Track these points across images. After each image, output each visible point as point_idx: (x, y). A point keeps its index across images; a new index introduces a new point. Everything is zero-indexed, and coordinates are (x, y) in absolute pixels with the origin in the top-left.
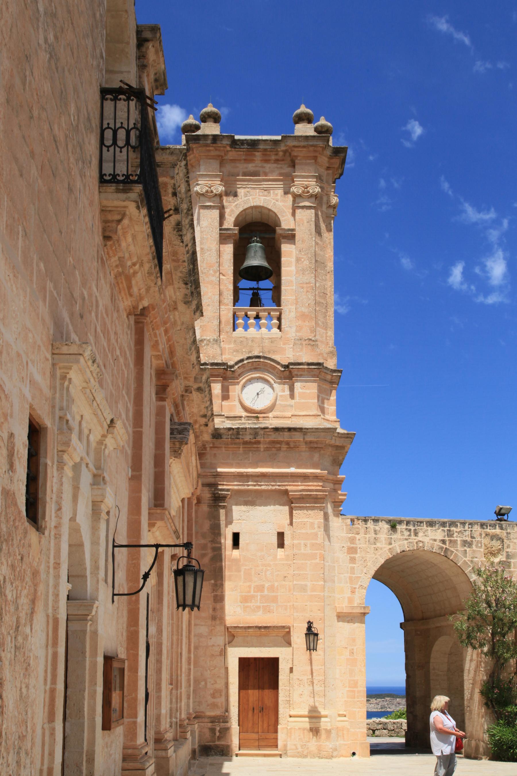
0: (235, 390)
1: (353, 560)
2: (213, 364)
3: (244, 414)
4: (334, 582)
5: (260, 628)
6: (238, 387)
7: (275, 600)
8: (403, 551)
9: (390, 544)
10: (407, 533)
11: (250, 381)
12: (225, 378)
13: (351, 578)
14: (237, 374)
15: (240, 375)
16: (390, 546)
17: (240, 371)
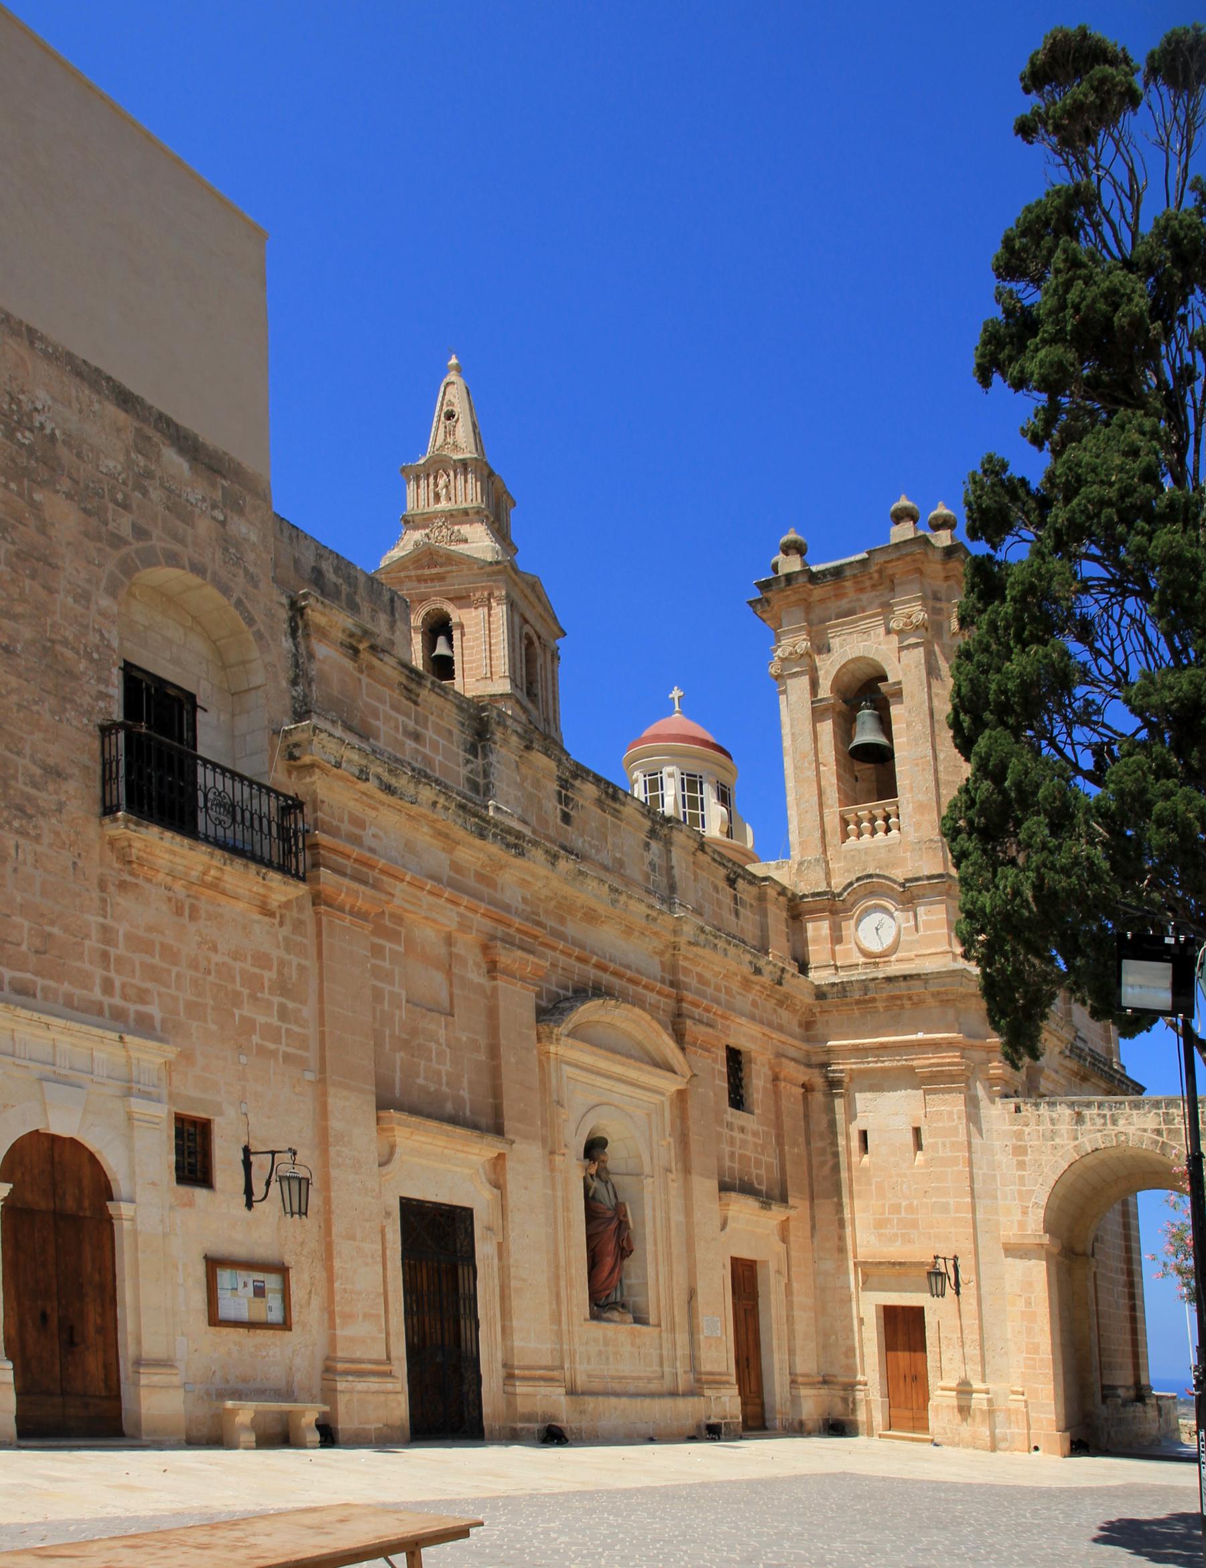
0: (848, 927)
1: (1021, 1165)
2: (814, 895)
3: (862, 960)
4: (996, 1198)
5: (894, 1264)
6: (852, 922)
7: (914, 1224)
8: (1097, 1149)
9: (1076, 1139)
10: (1100, 1121)
11: (867, 912)
12: (834, 912)
13: (1020, 1192)
14: (848, 904)
15: (853, 905)
16: (1076, 1143)
17: (851, 899)
